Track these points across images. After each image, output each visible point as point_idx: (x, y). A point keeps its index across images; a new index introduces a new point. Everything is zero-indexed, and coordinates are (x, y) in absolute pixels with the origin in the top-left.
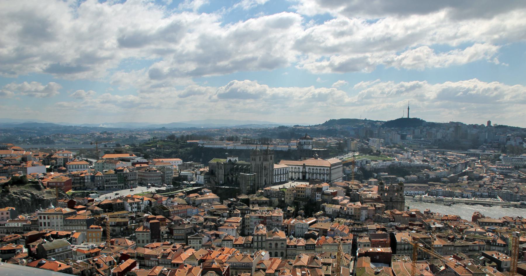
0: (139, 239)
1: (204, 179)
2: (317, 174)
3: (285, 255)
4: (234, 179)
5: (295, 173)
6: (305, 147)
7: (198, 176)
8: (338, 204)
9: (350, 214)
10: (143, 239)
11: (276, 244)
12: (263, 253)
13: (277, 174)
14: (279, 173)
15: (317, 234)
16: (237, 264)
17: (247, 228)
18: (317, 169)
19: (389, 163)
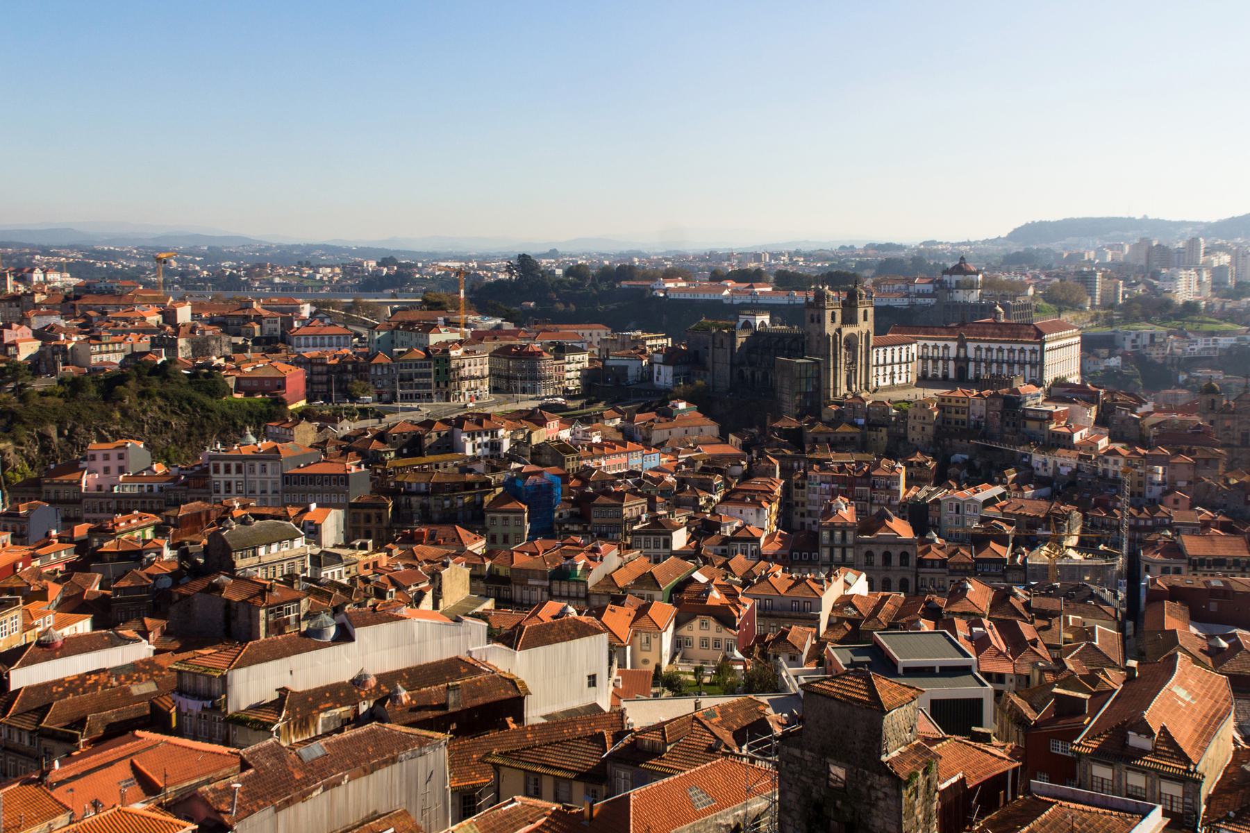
0: (493, 530)
1: (674, 375)
2: (1000, 363)
3: (912, 587)
4: (759, 375)
5: (935, 360)
6: (960, 296)
7: (656, 366)
9: (1111, 475)
10: (506, 530)
11: (887, 557)
12: (851, 576)
14: (889, 360)
15: (1009, 530)
16: (777, 602)
17: (799, 509)
18: (1000, 350)
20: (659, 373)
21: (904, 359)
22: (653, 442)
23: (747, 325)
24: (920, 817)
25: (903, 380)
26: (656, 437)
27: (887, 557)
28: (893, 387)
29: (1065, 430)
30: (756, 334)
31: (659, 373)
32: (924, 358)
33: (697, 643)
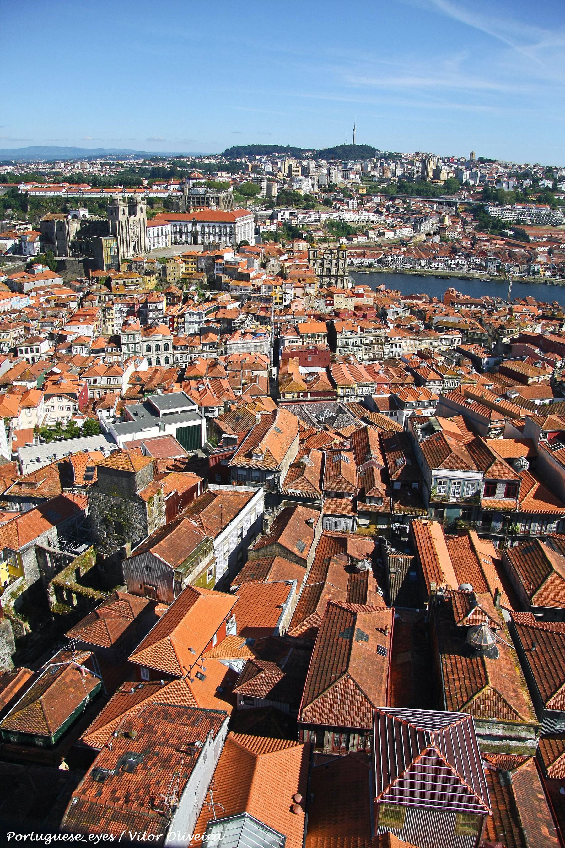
8: (249, 280)
11: (158, 348)
13: (152, 236)
14: (156, 235)
17: (111, 323)
19: (324, 216)
20: (25, 247)
21: (164, 234)
22: (25, 290)
23: (75, 217)
24: (156, 515)
25: (164, 245)
26: (27, 287)
27: (158, 348)
28: (158, 249)
29: (246, 272)
30: (83, 222)
31: (25, 247)
32: (175, 233)
33: (57, 408)
